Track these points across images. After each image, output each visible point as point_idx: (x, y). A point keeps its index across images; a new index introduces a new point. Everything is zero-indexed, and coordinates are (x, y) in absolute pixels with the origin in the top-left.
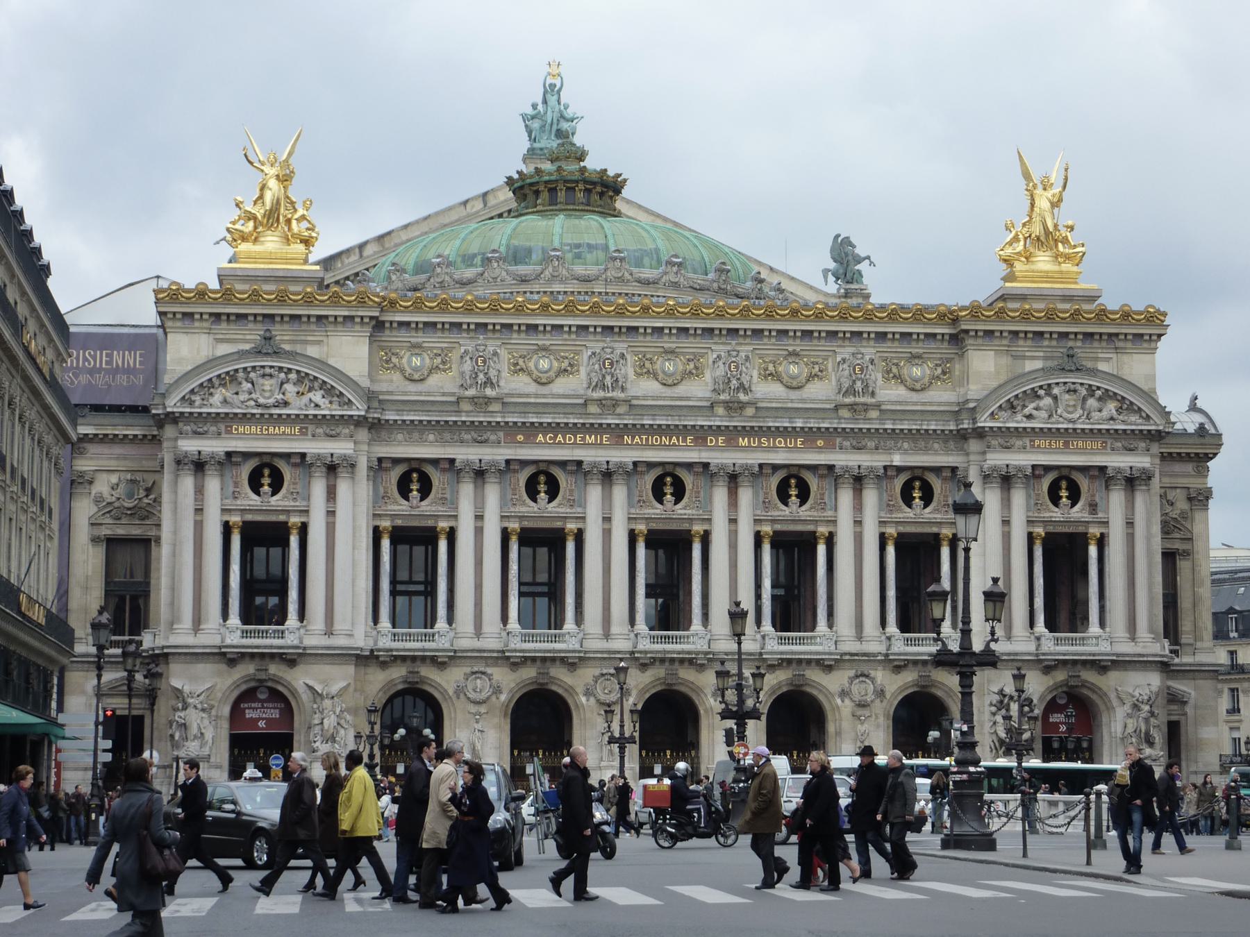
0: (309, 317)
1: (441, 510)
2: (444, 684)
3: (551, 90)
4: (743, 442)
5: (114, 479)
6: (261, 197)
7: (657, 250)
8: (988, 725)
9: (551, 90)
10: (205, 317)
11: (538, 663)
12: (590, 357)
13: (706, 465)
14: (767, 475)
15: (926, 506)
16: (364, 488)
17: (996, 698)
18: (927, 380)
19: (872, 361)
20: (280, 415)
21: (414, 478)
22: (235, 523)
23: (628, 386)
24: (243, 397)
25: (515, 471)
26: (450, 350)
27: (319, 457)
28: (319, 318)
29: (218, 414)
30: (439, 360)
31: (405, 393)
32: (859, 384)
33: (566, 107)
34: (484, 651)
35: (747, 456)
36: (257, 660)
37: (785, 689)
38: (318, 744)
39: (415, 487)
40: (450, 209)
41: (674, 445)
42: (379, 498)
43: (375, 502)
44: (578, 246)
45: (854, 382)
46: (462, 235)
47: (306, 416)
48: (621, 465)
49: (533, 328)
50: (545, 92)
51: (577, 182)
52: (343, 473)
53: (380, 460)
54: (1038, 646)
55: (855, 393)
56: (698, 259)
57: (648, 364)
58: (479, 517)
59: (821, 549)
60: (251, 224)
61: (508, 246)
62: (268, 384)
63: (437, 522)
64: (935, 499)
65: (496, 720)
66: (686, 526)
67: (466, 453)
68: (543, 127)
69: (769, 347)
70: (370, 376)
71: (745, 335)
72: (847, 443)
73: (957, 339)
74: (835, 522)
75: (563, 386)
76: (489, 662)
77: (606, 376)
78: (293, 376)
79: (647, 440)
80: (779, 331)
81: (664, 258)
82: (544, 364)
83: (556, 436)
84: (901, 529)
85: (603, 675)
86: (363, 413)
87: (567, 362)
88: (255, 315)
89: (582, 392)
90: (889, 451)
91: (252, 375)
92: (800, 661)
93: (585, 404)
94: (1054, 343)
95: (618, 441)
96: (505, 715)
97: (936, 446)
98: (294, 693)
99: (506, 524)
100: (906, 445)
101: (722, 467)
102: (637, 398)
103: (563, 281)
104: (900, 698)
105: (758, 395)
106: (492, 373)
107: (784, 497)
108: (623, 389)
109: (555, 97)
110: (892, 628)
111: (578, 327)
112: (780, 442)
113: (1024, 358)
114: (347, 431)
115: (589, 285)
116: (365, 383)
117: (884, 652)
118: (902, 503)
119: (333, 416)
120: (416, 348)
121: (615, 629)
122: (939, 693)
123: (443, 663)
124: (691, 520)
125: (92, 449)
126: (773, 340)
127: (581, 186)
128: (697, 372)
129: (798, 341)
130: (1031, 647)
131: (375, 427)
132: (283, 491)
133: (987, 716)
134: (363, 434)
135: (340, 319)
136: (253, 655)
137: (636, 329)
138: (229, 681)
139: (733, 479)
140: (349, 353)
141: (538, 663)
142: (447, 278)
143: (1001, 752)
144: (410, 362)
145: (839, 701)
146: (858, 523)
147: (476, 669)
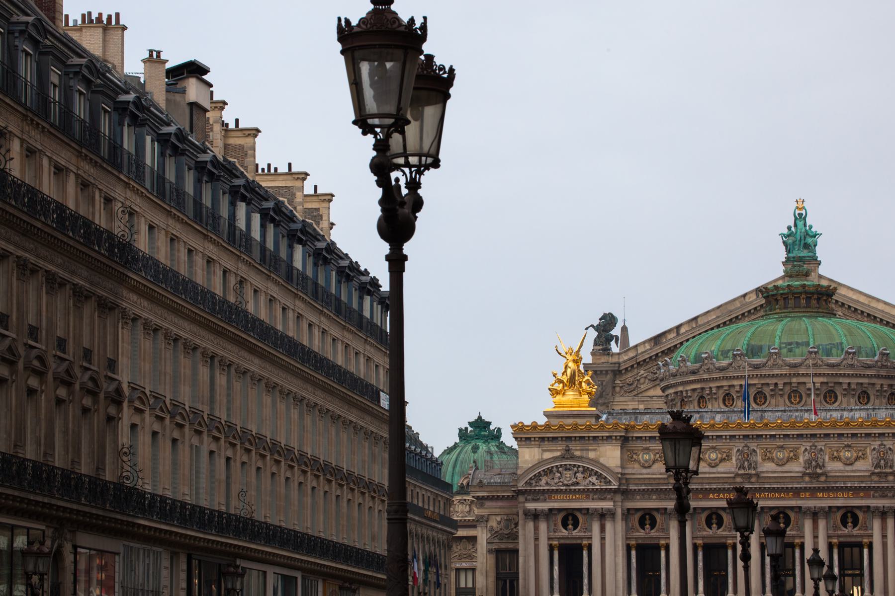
3: (800, 217)
4: (820, 495)
5: (499, 519)
6: (566, 371)
7: (841, 343)
9: (800, 217)
13: (800, 508)
16: (620, 525)
19: (890, 449)
24: (556, 480)
27: (596, 510)
28: (594, 438)
31: (641, 474)
32: (882, 462)
33: (811, 227)
39: (648, 522)
40: (734, 300)
42: (628, 529)
44: (790, 344)
46: (722, 337)
50: (796, 219)
51: (801, 293)
53: (628, 510)
55: (880, 467)
56: (869, 346)
60: (561, 385)
61: (748, 345)
62: (568, 474)
68: (794, 242)
69: (834, 443)
70: (622, 467)
71: (820, 437)
72: (876, 494)
74: (871, 536)
75: (722, 468)
80: (839, 434)
81: (846, 349)
82: (713, 456)
87: (725, 455)
89: (733, 470)
93: (734, 478)
101: (809, 508)
102: (763, 472)
103: (780, 367)
105: (829, 469)
107: (844, 523)
108: (755, 469)
109: (802, 222)
111: (730, 436)
112: (840, 494)
114: (609, 496)
115: (796, 369)
116: (620, 470)
125: (488, 503)
127: (803, 296)
128: (796, 457)
131: (625, 493)
132: (579, 528)
134: (618, 497)
137: (761, 435)
140: (610, 456)
142: (712, 367)
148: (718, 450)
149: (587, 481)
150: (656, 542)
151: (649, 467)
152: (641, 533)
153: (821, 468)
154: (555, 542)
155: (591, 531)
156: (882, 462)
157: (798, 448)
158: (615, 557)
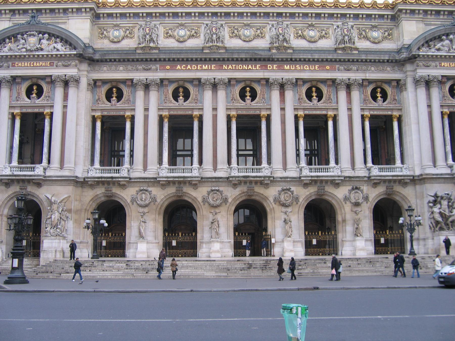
0: (59, 9)
1: (126, 106)
2: (125, 197)
4: (287, 67)
8: (427, 215)
10: (7, 12)
11: (177, 185)
12: (205, 27)
13: (267, 80)
14: (300, 86)
15: (384, 101)
17: (433, 198)
18: (380, 38)
20: (38, 55)
21: (115, 91)
22: (17, 114)
23: (226, 42)
24: (19, 47)
25: (167, 86)
26: (134, 27)
27: (58, 77)
28: (65, 10)
29: (7, 56)
30: (128, 32)
34: (147, 178)
35: (290, 73)
36: (21, 184)
37: (313, 198)
38: (48, 229)
39: (115, 95)
41: (250, 69)
43: (93, 103)
45: (344, 37)
47: (52, 55)
48: (221, 80)
49: (175, 15)
52: (71, 84)
53: (95, 81)
54: (452, 170)
57: (236, 31)
58: (146, 110)
59: (330, 123)
63: (125, 113)
64: (389, 97)
65: (153, 216)
66: (258, 112)
67: (139, 75)
69: (299, 23)
70: (91, 40)
71: (286, 16)
73: (394, 18)
74: (337, 109)
76: (150, 184)
77: (214, 37)
78: (46, 36)
79: (235, 67)
82: (182, 33)
83: (187, 66)
84: (372, 113)
85: (212, 190)
86: (81, 52)
87: (193, 31)
88: (32, 10)
89: (202, 46)
90: (365, 71)
91: (25, 36)
92: (322, 181)
94: (446, 17)
95: (220, 69)
96: (159, 214)
97: (388, 69)
98: (41, 200)
99: (161, 113)
100: (373, 69)
101: (275, 80)
104: (376, 201)
105: (294, 46)
106: (154, 36)
107: (309, 97)
110: (370, 164)
112: (306, 67)
113: (431, 25)
114: (74, 63)
116: (86, 41)
117: (367, 175)
118: (371, 100)
119: (66, 55)
120: (117, 27)
121: (219, 167)
122: (397, 198)
123: (124, 185)
124: (260, 109)
126: (301, 19)
129: (313, 19)
130: (448, 171)
132: (43, 96)
133: (426, 208)
134: (84, 66)
135: (74, 10)
136: (18, 181)
138: (7, 195)
139: (282, 87)
141: (177, 185)
143: (437, 229)
144: (113, 34)
145: (344, 203)
146: (350, 109)
147: (142, 188)
148: (186, 27)
149: (52, 47)
150: (122, 113)
151: (119, 42)
152: (107, 105)
153: (287, 43)
154: (17, 111)
155: (53, 100)
156: (347, 37)
157: (264, 27)
158: (77, 125)
